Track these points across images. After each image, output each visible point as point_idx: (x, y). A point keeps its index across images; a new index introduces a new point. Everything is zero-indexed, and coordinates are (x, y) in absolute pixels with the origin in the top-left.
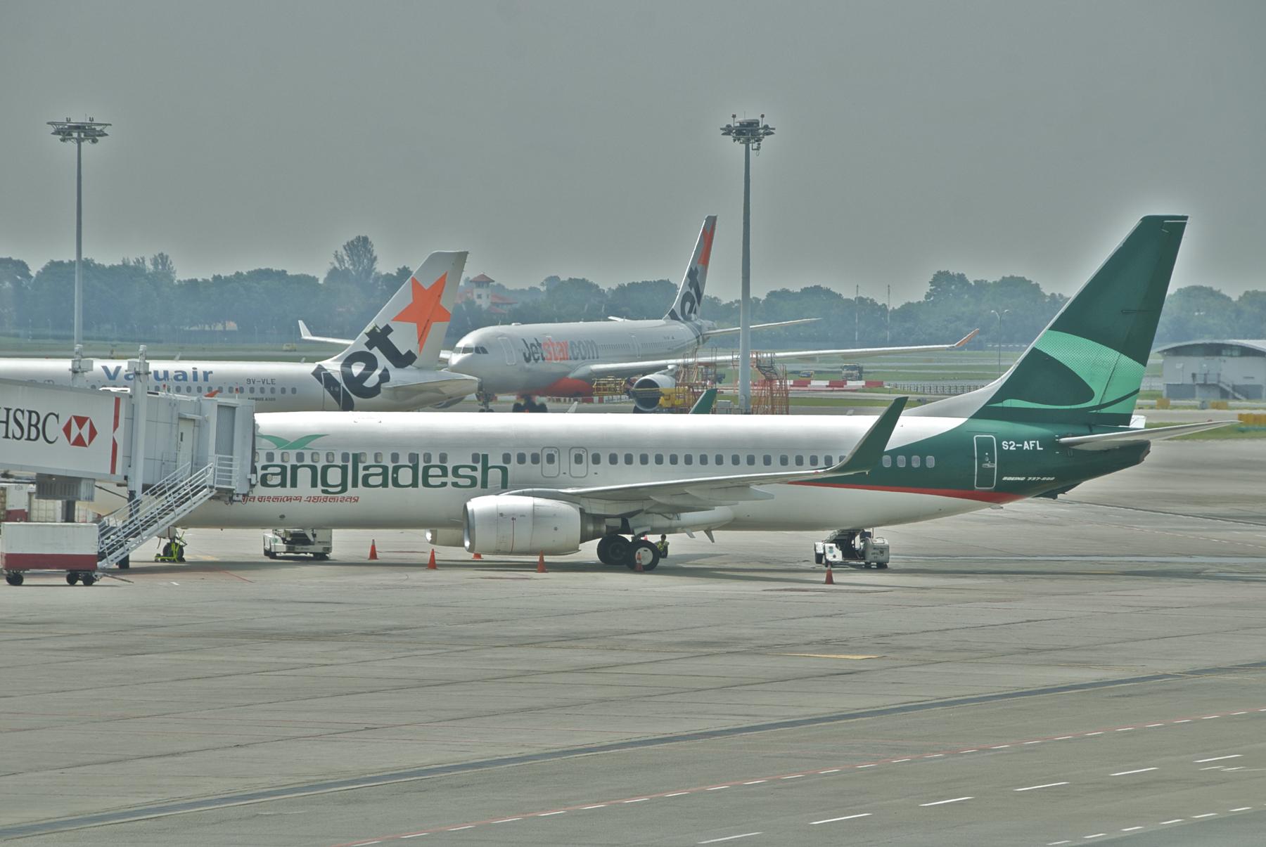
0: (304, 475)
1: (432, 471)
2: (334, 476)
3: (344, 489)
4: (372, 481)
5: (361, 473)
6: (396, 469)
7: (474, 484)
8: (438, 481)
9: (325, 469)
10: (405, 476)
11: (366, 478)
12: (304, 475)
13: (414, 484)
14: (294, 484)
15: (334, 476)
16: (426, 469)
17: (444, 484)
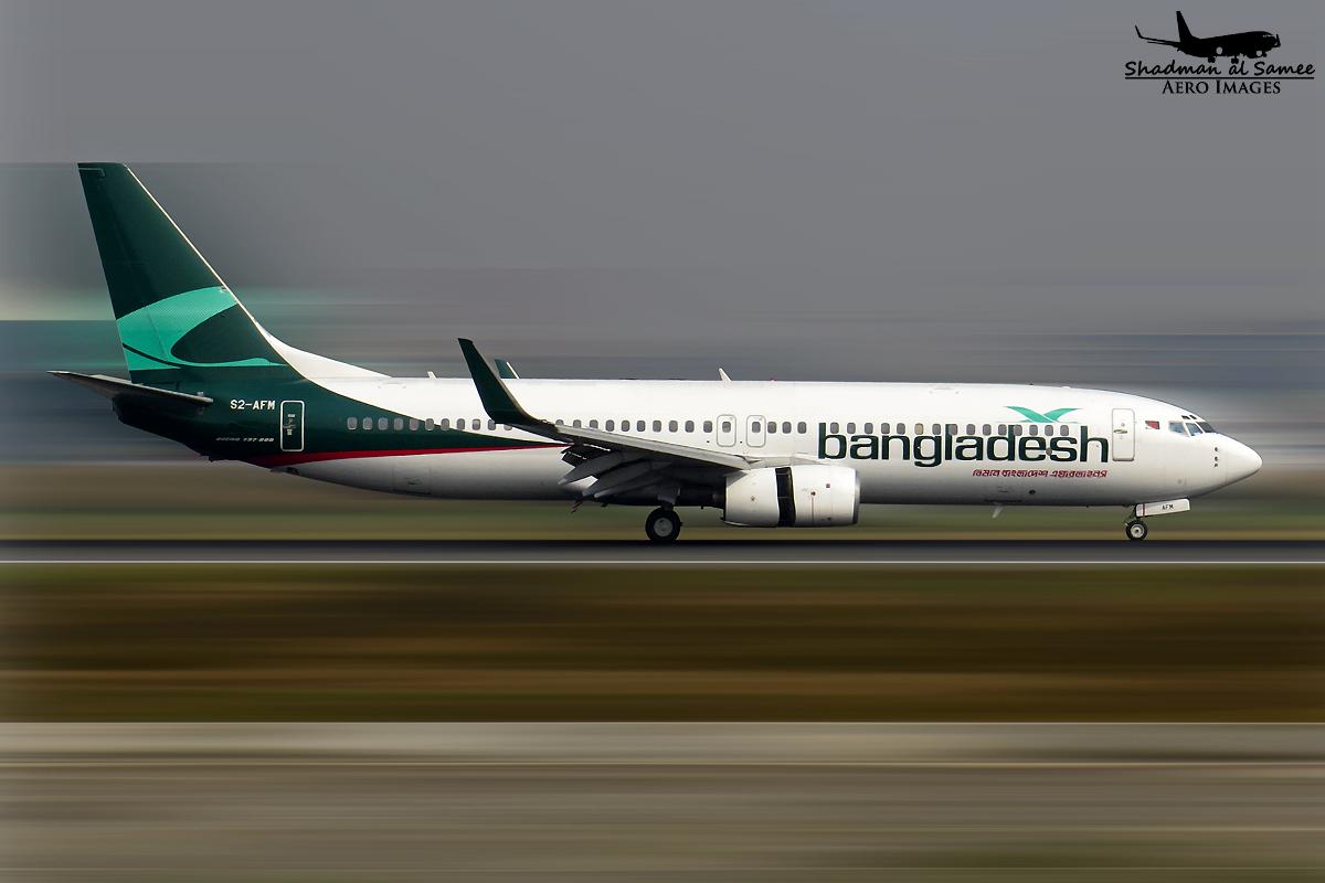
0: (896, 446)
1: (1029, 444)
2: (928, 448)
3: (938, 462)
4: (966, 452)
5: (955, 445)
6: (992, 441)
7: (1073, 457)
8: (1036, 454)
9: (918, 441)
10: (1001, 448)
11: (960, 449)
12: (896, 446)
13: (1011, 457)
14: (886, 456)
15: (928, 448)
16: (1023, 441)
17: (1042, 458)
